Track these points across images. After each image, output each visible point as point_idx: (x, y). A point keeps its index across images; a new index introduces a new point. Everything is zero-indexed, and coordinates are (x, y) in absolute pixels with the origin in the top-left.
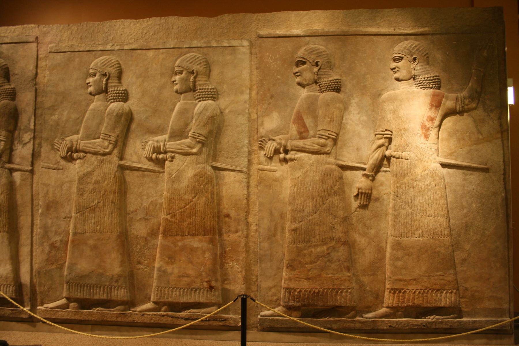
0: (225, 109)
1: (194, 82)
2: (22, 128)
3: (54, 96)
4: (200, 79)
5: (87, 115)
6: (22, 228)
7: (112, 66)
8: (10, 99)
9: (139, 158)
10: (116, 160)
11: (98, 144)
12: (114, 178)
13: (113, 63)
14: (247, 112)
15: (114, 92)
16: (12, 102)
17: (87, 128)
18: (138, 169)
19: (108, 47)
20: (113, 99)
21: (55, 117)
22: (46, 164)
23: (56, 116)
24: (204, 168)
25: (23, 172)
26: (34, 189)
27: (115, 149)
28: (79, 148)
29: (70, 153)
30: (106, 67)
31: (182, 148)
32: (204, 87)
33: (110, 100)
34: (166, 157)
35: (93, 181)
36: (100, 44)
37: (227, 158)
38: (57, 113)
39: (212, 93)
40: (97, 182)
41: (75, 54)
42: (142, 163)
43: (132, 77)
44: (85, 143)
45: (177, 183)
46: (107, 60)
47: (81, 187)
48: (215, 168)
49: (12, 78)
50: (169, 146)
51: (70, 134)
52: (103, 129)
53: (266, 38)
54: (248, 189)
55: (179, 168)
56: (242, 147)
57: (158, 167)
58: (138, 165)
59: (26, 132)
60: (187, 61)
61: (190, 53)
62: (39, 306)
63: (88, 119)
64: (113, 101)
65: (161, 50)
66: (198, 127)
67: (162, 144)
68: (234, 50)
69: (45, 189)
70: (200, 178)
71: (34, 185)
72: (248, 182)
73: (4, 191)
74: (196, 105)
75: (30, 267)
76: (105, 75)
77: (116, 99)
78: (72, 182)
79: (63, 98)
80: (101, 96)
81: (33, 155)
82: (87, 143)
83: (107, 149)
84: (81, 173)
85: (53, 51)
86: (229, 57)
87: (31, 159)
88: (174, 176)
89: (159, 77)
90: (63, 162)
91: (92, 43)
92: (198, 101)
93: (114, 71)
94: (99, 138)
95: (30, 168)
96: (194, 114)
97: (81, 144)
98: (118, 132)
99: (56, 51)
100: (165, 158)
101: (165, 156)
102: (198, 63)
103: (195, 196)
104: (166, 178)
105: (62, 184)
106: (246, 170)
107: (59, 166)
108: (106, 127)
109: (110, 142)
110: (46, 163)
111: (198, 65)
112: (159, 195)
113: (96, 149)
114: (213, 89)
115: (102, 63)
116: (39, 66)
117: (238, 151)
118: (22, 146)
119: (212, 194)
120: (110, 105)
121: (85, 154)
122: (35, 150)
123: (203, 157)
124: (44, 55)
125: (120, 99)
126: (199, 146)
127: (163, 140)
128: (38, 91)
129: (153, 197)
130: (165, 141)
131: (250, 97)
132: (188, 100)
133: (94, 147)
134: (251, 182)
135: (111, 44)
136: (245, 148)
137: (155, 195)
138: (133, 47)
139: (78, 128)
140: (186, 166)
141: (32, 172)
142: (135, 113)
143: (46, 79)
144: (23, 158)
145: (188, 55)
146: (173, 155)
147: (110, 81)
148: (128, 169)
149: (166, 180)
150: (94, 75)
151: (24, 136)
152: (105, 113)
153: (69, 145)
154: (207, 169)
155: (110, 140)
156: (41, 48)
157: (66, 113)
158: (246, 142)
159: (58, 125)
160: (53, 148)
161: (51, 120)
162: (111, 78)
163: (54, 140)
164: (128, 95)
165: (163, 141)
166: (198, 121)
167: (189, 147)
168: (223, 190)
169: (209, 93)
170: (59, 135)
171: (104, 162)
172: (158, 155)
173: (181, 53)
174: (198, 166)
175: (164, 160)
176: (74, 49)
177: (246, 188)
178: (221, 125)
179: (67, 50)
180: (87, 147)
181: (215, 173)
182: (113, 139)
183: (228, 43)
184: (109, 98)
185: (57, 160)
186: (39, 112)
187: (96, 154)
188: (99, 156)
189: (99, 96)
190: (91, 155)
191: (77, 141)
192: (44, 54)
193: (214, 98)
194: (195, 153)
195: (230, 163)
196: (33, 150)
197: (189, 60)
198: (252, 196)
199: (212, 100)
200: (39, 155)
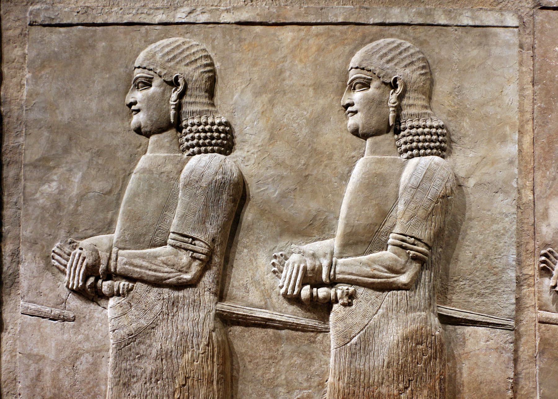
3: (46, 134)
7: (191, 62)
9: (266, 295)
10: (210, 301)
15: (200, 128)
18: (265, 324)
19: (180, 16)
20: (198, 145)
21: (51, 188)
22: (32, 306)
23: (54, 184)
27: (207, 274)
28: (115, 269)
29: (91, 280)
30: (177, 63)
33: (188, 148)
36: (157, 9)
38: (55, 177)
41: (95, 31)
42: (274, 309)
43: (242, 92)
46: (178, 46)
50: (343, 269)
51: (90, 232)
52: (175, 221)
57: (314, 318)
63: (135, 195)
64: (196, 149)
65: (314, 27)
67: (325, 263)
76: (174, 83)
77: (204, 145)
79: (70, 139)
80: (167, 137)
82: (136, 256)
83: (186, 272)
84: (123, 332)
89: (311, 92)
90: (75, 302)
94: (166, 244)
97: (119, 258)
99: (47, 23)
101: (332, 292)
104: (333, 345)
107: (66, 312)
108: (183, 217)
109: (195, 254)
112: (316, 384)
113: (160, 271)
115: (168, 53)
120: (188, 160)
121: (131, 285)
125: (216, 145)
127: (328, 251)
129: (301, 390)
130: (332, 254)
133: (154, 267)
135: (187, 9)
137: (305, 385)
138: (244, 16)
139: (110, 215)
146: (351, 289)
147: (186, 99)
148: (238, 324)
153: (89, 260)
155: (194, 251)
157: (77, 178)
159: (58, 206)
160: (48, 266)
162: (189, 93)
163: (51, 245)
164: (233, 137)
165: (328, 256)
171: (180, 305)
172: (315, 290)
176: (94, 18)
179: (75, 21)
180: (136, 266)
182: (200, 247)
184: (186, 144)
187: (158, 283)
188: (166, 290)
189: (162, 136)
190: (145, 286)
191: (110, 249)
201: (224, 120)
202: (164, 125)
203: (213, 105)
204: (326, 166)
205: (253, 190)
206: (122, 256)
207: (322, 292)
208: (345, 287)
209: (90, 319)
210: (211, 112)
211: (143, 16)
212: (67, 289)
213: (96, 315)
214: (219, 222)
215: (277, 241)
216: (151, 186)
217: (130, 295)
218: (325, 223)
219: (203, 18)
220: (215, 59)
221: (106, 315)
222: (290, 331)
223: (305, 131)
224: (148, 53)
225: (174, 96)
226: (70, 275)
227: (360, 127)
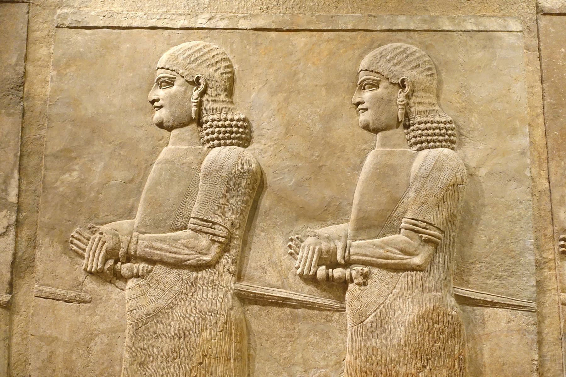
0: (478, 167)
1: (407, 106)
3: (69, 127)
4: (419, 100)
5: (152, 174)
11: (184, 241)
12: (226, 323)
13: (214, 56)
14: (529, 175)
15: (220, 123)
17: (154, 204)
18: (282, 303)
19: (201, 22)
23: (75, 174)
24: (442, 300)
26: (14, 348)
28: (135, 252)
29: (111, 262)
30: (198, 65)
31: (389, 254)
32: (430, 119)
33: (208, 141)
34: (351, 274)
35: (172, 330)
36: (180, 15)
37: (489, 277)
38: (77, 167)
39: (449, 132)
40: (183, 334)
43: (259, 91)
44: (150, 240)
45: (380, 337)
46: (200, 50)
47: (140, 345)
48: (463, 301)
50: (357, 251)
51: (110, 218)
52: (196, 207)
53: (557, 15)
54: (540, 349)
55: (381, 301)
56: (521, 254)
57: (330, 298)
58: (283, 294)
60: (389, 61)
61: (391, 41)
63: (157, 183)
64: (216, 142)
65: (325, 33)
66: (424, 207)
67: (340, 245)
68: (490, 39)
69: (43, 350)
70: (434, 323)
71: (14, 340)
72: (539, 333)
74: (413, 157)
77: (224, 139)
78: (115, 332)
79: (93, 132)
83: (206, 254)
84: (140, 313)
85: (67, 23)
86: (479, 54)
87: (9, 275)
88: (370, 319)
89: (324, 92)
90: (91, 285)
91: (160, 11)
92: (415, 148)
93: (217, 75)
94: (187, 229)
95: (6, 298)
96: (412, 177)
97: (140, 242)
98: (233, 216)
100: (348, 277)
101: (347, 272)
102: (414, 64)
103: (425, 367)
105: (91, 337)
106: (534, 305)
107: (82, 294)
108: (204, 204)
109: (215, 238)
111: (412, 68)
112: (333, 363)
113: (180, 254)
114: (450, 122)
115: (189, 56)
116: (30, 57)
117: (512, 261)
119: (462, 360)
120: (208, 152)
121: (150, 267)
122: (20, 253)
123: (436, 276)
126: (429, 249)
127: (342, 234)
128: (28, 114)
129: (318, 369)
130: (346, 237)
131: (532, 143)
132: (395, 146)
133: (174, 250)
134: (546, 331)
135: (208, 16)
136: (527, 255)
137: (322, 363)
138: (261, 23)
140: (398, 295)
141: (8, 306)
142: (265, 170)
143: (49, 89)
145: (389, 46)
146: (366, 269)
147: (206, 97)
148: (256, 303)
149: (349, 330)
150: (170, 83)
152: (198, 169)
153: (109, 244)
154: (449, 303)
155: (214, 235)
156: (35, 15)
157: (99, 167)
158: (530, 241)
159: (79, 194)
162: (209, 91)
163: (70, 230)
164: (251, 132)
165: (343, 239)
166: (423, 193)
167: (404, 252)
168: (484, 352)
169: (443, 131)
170: (82, 219)
171: (199, 285)
172: (330, 270)
173: (373, 42)
174: (427, 295)
175: (344, 283)
176: (120, 21)
177: (535, 346)
178: (472, 204)
180: (157, 249)
181: (464, 311)
183: (476, 25)
184: (206, 137)
185: (76, 278)
186: (31, 162)
187: (178, 265)
188: (186, 271)
189: (182, 130)
191: (130, 234)
192: (43, 30)
193: (453, 142)
194: (419, 266)
195: (496, 290)
196: (15, 254)
197: (393, 58)
198: (548, 364)
199: (448, 147)
201: (242, 116)
202: (186, 120)
203: (232, 103)
204: (339, 158)
205: (269, 179)
206: (143, 239)
207: (337, 273)
208: (359, 268)
209: (107, 300)
210: (230, 109)
211: (166, 20)
212: (83, 272)
213: (113, 296)
214: (239, 209)
215: (293, 226)
216: (173, 175)
217: (149, 277)
218: (339, 209)
219: (222, 24)
220: (233, 61)
221: (123, 297)
222: (307, 310)
223: (318, 126)
224: (171, 55)
225: (196, 94)
226: (88, 258)
227: (371, 122)
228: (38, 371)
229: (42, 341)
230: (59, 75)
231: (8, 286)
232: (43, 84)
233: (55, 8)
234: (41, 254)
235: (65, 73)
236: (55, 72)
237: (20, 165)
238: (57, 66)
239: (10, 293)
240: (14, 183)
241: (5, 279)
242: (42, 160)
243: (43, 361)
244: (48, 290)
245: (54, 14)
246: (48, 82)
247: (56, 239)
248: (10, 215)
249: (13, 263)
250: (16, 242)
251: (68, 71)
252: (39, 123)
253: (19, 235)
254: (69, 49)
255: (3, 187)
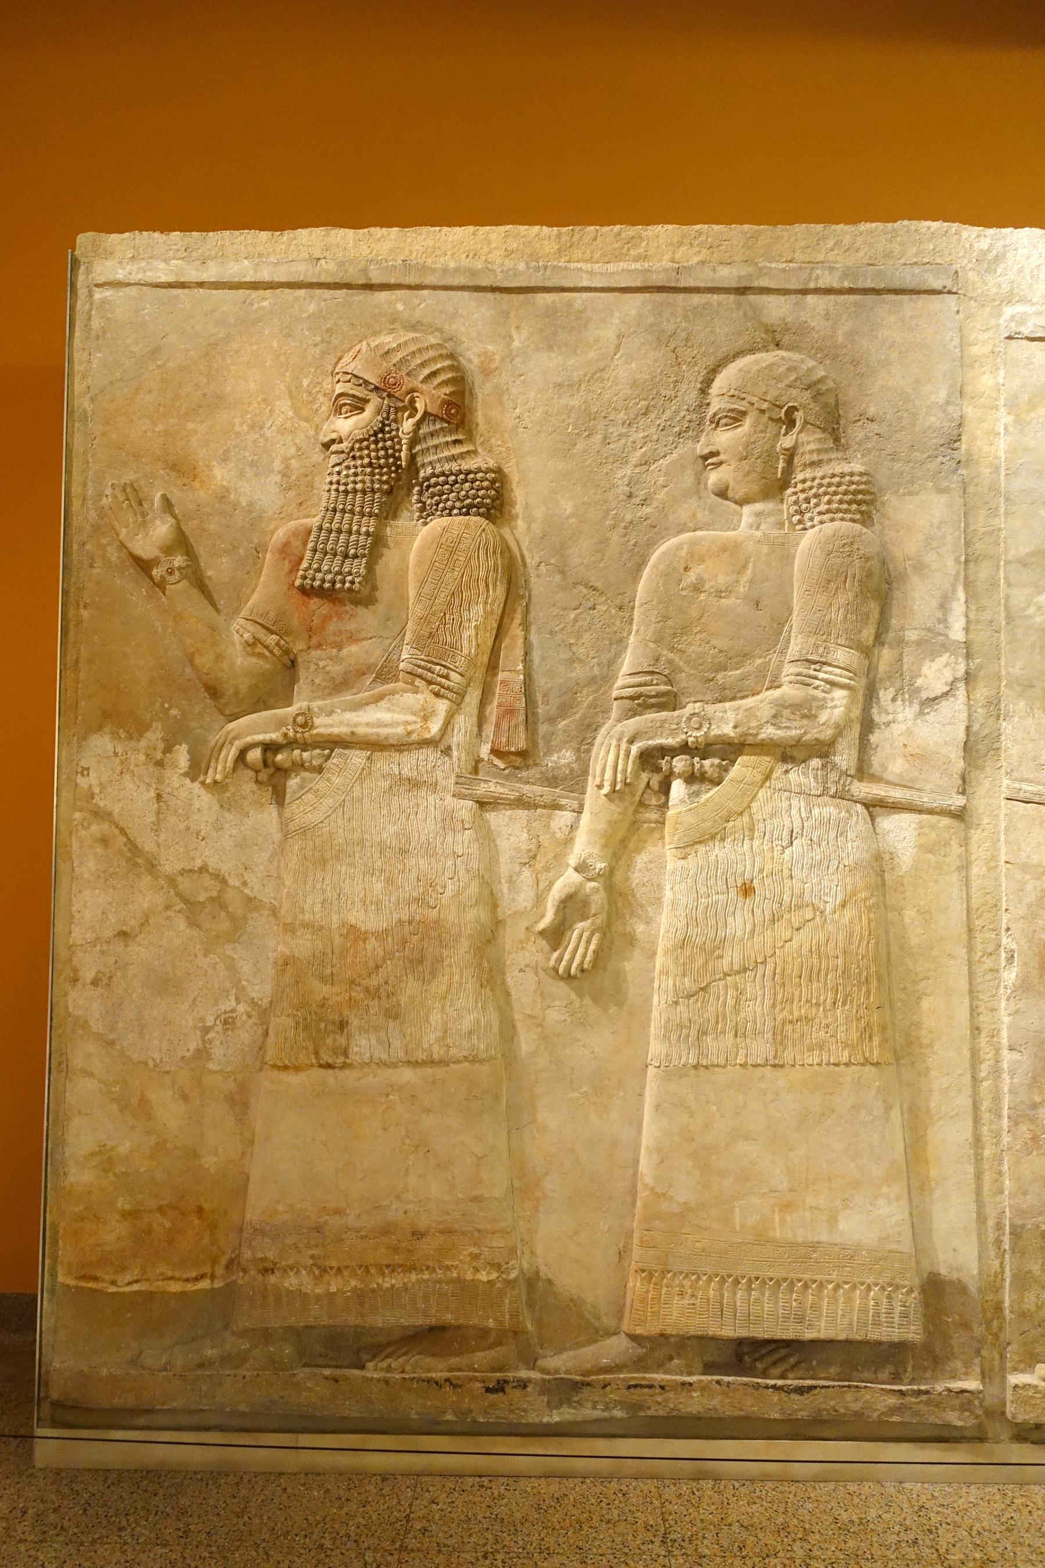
2: (912, 635)
6: (931, 1045)
8: (858, 516)
16: (865, 530)
25: (924, 816)
26: (975, 885)
49: (856, 433)
59: (933, 655)
62: (1015, 1369)
69: (1029, 887)
71: (975, 871)
73: (854, 893)
75: (973, 1207)
81: (968, 748)
85: (1026, 331)
95: (960, 801)
110: (1026, 780)
118: (916, 707)
122: (976, 727)
124: (987, 349)
128: (971, 489)
143: (1001, 446)
144: (920, 758)
151: (925, 670)
161: (1039, 608)
196: (968, 728)
200: (995, 749)
228: (1022, 921)
229: (1025, 873)
230: (1018, 421)
231: (960, 782)
232: (991, 438)
233: (1000, 305)
234: (1013, 728)
235: (1028, 419)
236: (1011, 418)
237: (966, 578)
238: (1012, 406)
239: (963, 793)
240: (958, 607)
241: (955, 770)
242: (998, 569)
243: (1029, 906)
244: (1029, 788)
245: (999, 315)
246: (999, 434)
247: (1038, 705)
248: (956, 663)
249: (965, 743)
250: (970, 707)
251: (1033, 415)
252: (987, 506)
253: (972, 697)
254: (1032, 377)
255: (940, 615)
